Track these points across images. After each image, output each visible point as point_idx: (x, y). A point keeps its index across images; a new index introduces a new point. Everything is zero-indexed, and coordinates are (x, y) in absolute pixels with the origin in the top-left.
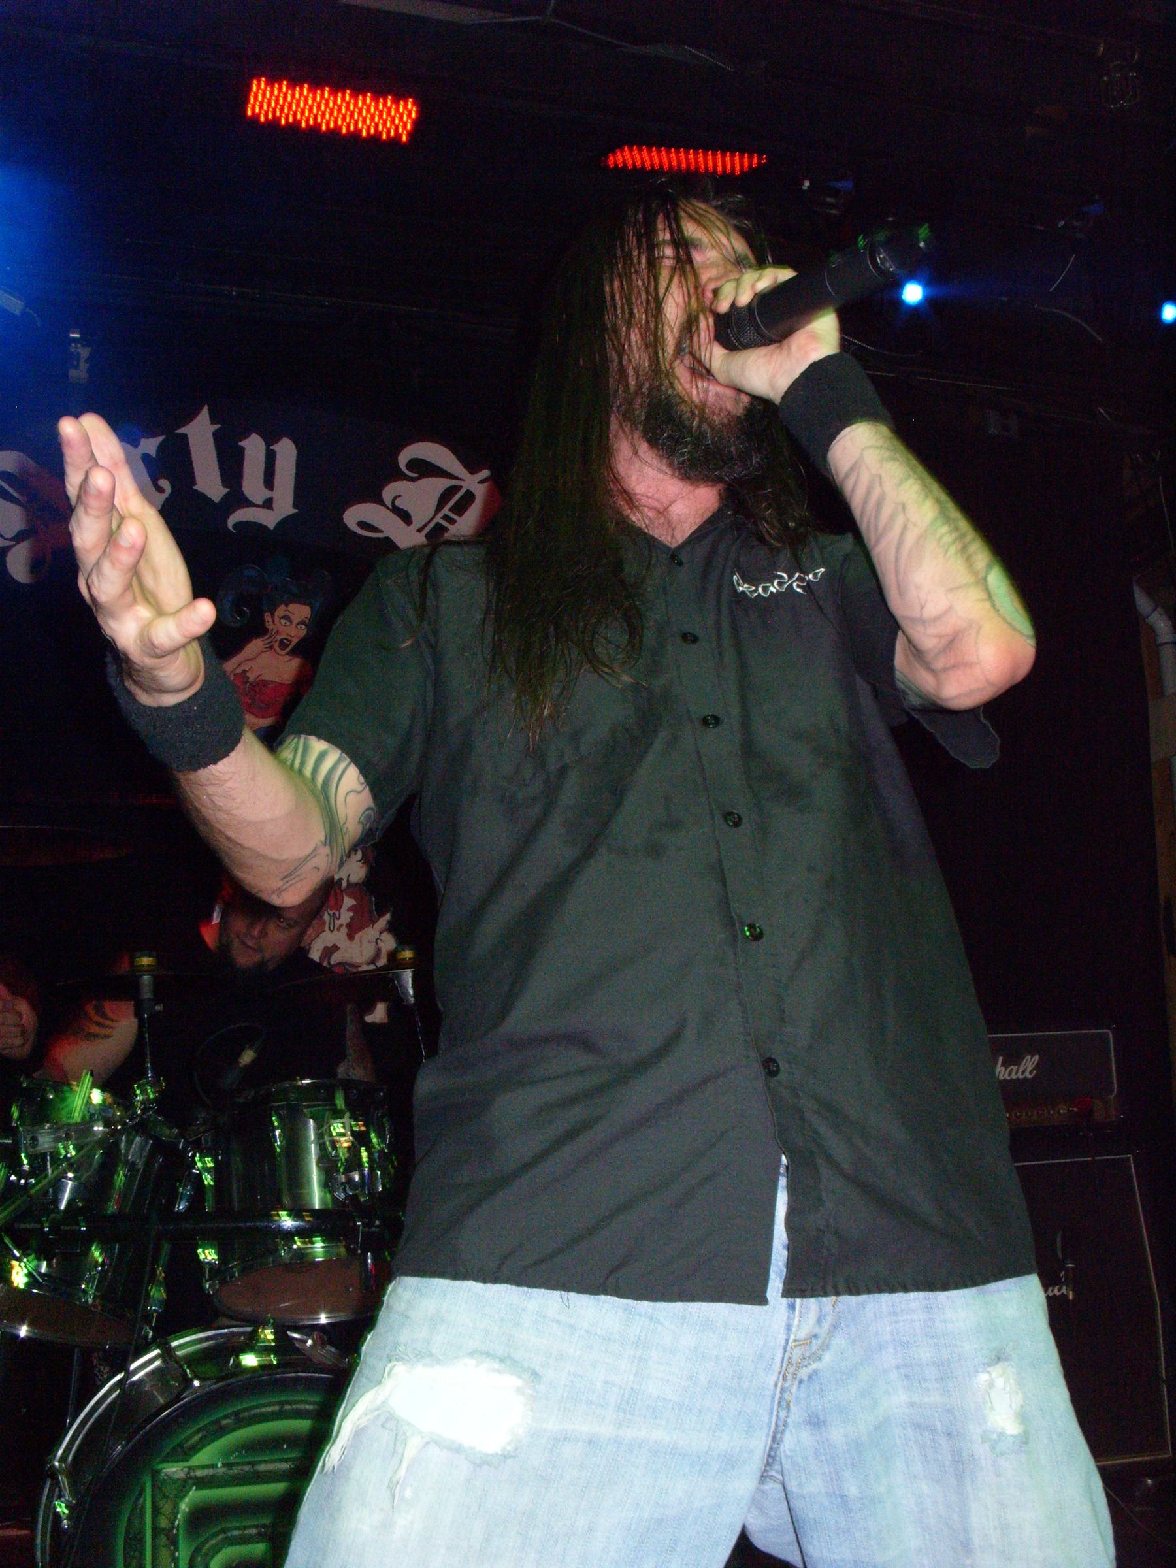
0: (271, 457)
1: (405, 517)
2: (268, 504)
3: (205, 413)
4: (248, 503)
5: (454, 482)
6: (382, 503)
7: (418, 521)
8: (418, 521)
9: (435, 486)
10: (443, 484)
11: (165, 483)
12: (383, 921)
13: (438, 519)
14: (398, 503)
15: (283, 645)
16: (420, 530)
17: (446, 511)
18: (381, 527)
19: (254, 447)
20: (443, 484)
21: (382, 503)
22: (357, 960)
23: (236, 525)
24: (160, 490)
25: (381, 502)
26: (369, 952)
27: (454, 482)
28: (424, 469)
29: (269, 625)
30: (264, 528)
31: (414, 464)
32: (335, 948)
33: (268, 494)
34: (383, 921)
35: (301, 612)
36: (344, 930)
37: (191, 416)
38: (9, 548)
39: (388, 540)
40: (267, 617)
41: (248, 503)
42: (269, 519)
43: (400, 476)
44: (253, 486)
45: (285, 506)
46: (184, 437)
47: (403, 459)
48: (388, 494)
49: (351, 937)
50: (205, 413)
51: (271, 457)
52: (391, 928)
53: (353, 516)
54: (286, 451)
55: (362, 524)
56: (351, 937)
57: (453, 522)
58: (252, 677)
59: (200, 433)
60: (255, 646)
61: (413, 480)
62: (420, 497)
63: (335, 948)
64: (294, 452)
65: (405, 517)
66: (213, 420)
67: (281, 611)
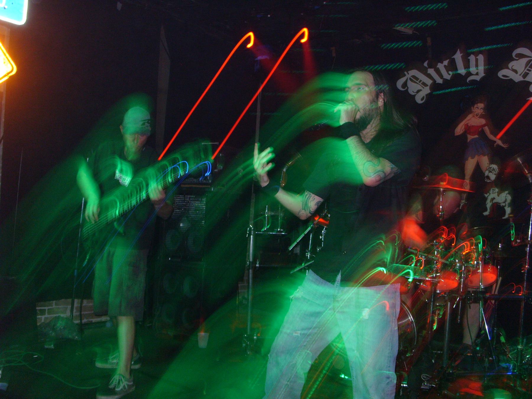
0: (477, 60)
1: (516, 71)
2: (477, 74)
4: (473, 75)
5: (530, 59)
7: (519, 73)
8: (519, 73)
9: (524, 61)
10: (527, 59)
13: (526, 71)
14: (514, 68)
15: (477, 115)
17: (528, 68)
19: (472, 58)
20: (527, 59)
21: (509, 69)
22: (500, 202)
25: (508, 68)
26: (504, 200)
27: (530, 59)
28: (521, 56)
32: (494, 198)
33: (477, 71)
35: (481, 105)
36: (496, 194)
37: (455, 53)
38: (415, 95)
39: (511, 80)
40: (472, 108)
41: (473, 75)
42: (478, 78)
43: (513, 60)
45: (482, 74)
46: (454, 58)
47: (514, 54)
48: (510, 65)
49: (498, 196)
51: (477, 60)
52: (509, 193)
53: (501, 74)
55: (504, 76)
56: (498, 196)
57: (530, 71)
58: (469, 125)
59: (458, 57)
60: (470, 116)
61: (517, 60)
62: (519, 65)
63: (494, 198)
65: (516, 71)
67: (476, 106)
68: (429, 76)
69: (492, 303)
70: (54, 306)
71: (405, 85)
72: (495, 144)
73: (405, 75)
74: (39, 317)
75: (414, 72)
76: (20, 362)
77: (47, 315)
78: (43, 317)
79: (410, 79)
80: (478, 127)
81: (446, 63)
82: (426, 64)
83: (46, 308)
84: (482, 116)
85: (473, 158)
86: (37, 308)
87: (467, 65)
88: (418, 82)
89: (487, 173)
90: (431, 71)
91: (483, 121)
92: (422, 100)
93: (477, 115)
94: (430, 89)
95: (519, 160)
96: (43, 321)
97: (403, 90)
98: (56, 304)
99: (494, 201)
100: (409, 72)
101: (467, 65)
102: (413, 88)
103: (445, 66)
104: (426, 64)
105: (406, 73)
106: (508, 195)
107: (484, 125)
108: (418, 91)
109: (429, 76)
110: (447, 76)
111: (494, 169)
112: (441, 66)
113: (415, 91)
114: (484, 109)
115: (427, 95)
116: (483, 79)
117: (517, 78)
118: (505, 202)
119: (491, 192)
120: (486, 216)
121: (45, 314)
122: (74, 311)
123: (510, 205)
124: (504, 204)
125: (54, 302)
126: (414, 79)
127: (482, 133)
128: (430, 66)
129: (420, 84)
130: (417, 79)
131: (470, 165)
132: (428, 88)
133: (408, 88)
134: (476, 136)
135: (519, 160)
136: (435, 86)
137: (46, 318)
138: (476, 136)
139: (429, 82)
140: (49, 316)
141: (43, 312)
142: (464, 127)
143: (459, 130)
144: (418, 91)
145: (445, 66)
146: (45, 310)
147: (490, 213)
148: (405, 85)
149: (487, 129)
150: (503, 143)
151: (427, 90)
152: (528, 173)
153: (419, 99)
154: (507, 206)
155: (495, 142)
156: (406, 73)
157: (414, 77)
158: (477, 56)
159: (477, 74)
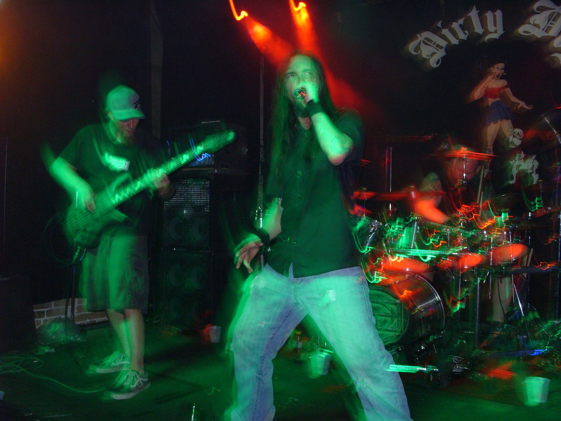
0: (495, 17)
2: (496, 32)
3: (474, 8)
6: (530, 23)
7: (542, 27)
9: (547, 13)
11: (466, 32)
12: (534, 157)
14: (535, 22)
16: (543, 30)
18: (530, 31)
23: (487, 40)
24: (465, 34)
25: (530, 23)
29: (493, 71)
30: (496, 39)
31: (537, 9)
32: (520, 165)
34: (534, 157)
35: (501, 65)
39: (533, 35)
44: (491, 28)
45: (500, 31)
46: (470, 17)
50: (474, 8)
51: (495, 17)
52: (536, 159)
53: (521, 30)
54: (499, 13)
55: (525, 32)
59: (474, 14)
60: (490, 78)
64: (501, 13)
66: (477, 10)
67: (496, 66)
68: (444, 37)
69: (523, 276)
70: (53, 307)
71: (417, 48)
72: (519, 107)
73: (417, 38)
74: (38, 319)
75: (427, 34)
76: (18, 369)
77: (46, 318)
78: (42, 320)
79: (424, 42)
80: (500, 89)
81: (461, 21)
82: (439, 25)
83: (45, 310)
84: (502, 77)
85: (495, 122)
86: (34, 310)
87: (483, 23)
88: (432, 44)
89: (511, 139)
90: (445, 32)
91: (503, 83)
92: (437, 63)
93: (498, 77)
94: (446, 50)
95: (547, 120)
96: (42, 324)
97: (415, 53)
98: (56, 305)
99: (521, 168)
100: (422, 34)
101: (483, 23)
102: (425, 51)
103: (460, 25)
104: (439, 25)
105: (418, 35)
106: (535, 161)
107: (506, 87)
108: (433, 54)
109: (444, 37)
110: (463, 36)
111: (518, 134)
112: (455, 25)
113: (430, 54)
114: (506, 69)
115: (441, 58)
116: (501, 36)
117: (539, 34)
118: (532, 169)
119: (517, 158)
120: (513, 185)
121: (44, 317)
122: (75, 311)
123: (538, 171)
124: (531, 171)
125: (53, 302)
126: (427, 42)
127: (503, 97)
128: (445, 26)
129: (434, 46)
130: (431, 41)
131: (491, 130)
132: (443, 50)
133: (421, 51)
134: (498, 99)
135: (547, 120)
136: (450, 49)
137: (45, 321)
138: (498, 99)
139: (443, 43)
140: (48, 318)
141: (41, 314)
142: (483, 91)
143: (477, 93)
144: (433, 54)
145: (460, 25)
146: (43, 312)
147: (516, 181)
148: (417, 48)
149: (508, 90)
150: (527, 105)
151: (441, 53)
152: (558, 133)
153: (433, 63)
154: (535, 173)
155: (519, 104)
156: (418, 35)
157: (426, 39)
158: (496, 11)
159: (496, 32)
